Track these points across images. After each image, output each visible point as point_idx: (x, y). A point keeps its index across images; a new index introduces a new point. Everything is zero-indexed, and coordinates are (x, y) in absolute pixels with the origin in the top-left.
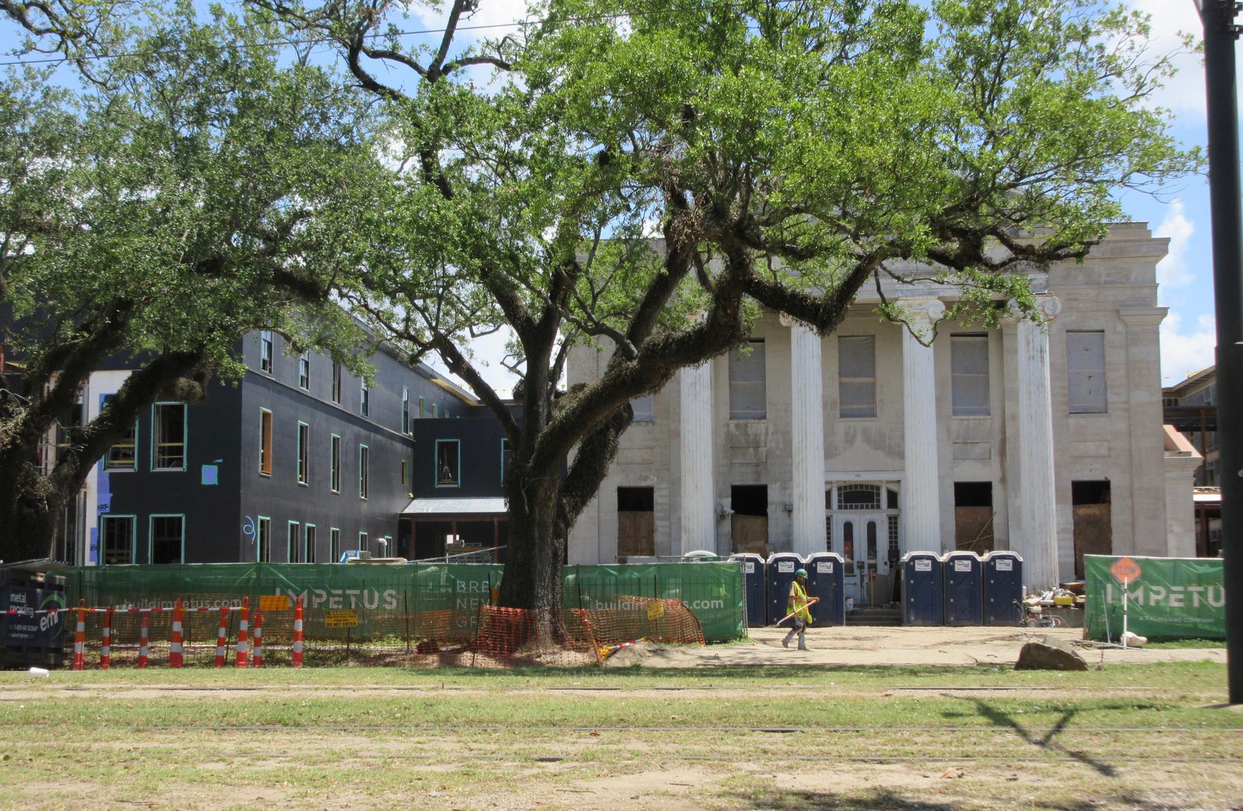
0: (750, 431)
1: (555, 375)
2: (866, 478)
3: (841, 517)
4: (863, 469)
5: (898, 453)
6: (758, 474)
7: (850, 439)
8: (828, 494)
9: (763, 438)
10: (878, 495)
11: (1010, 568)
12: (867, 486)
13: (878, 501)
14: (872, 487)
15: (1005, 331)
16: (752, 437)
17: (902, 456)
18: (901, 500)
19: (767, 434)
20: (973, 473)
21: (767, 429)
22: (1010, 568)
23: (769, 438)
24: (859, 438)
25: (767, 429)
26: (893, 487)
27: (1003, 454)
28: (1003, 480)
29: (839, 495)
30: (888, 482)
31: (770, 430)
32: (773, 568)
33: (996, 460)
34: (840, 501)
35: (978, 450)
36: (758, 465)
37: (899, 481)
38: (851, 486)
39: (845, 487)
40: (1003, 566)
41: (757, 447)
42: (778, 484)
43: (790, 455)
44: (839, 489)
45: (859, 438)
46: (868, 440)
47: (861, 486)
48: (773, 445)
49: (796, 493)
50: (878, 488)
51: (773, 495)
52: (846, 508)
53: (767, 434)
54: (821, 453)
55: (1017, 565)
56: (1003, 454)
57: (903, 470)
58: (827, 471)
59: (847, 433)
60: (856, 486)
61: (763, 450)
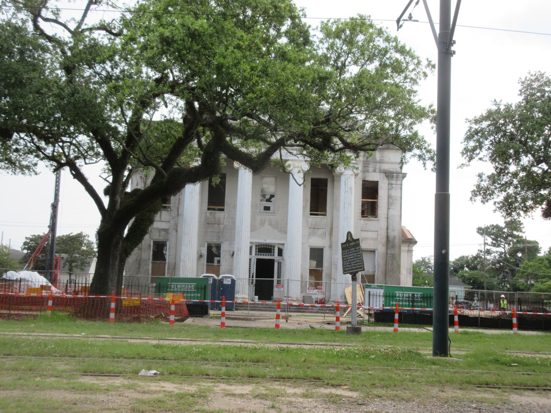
0: (216, 216)
1: (125, 185)
2: (269, 241)
4: (268, 238)
5: (283, 229)
6: (219, 237)
7: (262, 223)
8: (251, 248)
9: (222, 220)
10: (274, 250)
11: (230, 283)
12: (269, 246)
13: (274, 252)
14: (271, 246)
15: (335, 178)
16: (217, 219)
17: (285, 232)
18: (285, 253)
19: (224, 218)
20: (317, 242)
21: (224, 216)
22: (230, 283)
23: (225, 220)
24: (267, 223)
25: (224, 216)
26: (281, 247)
27: (331, 234)
28: (330, 247)
29: (256, 249)
30: (279, 244)
31: (226, 217)
32: (221, 281)
33: (328, 236)
34: (256, 252)
35: (320, 231)
36: (219, 233)
37: (284, 244)
38: (261, 245)
39: (259, 246)
40: (227, 282)
41: (219, 224)
42: (228, 242)
43: (235, 228)
44: (256, 246)
45: (267, 223)
46: (270, 224)
47: (266, 245)
48: (227, 223)
49: (236, 246)
50: (274, 247)
51: (224, 248)
53: (224, 218)
54: (249, 229)
55: (233, 281)
56: (331, 234)
57: (285, 239)
58: (251, 237)
59: (261, 220)
60: (264, 245)
61: (222, 226)
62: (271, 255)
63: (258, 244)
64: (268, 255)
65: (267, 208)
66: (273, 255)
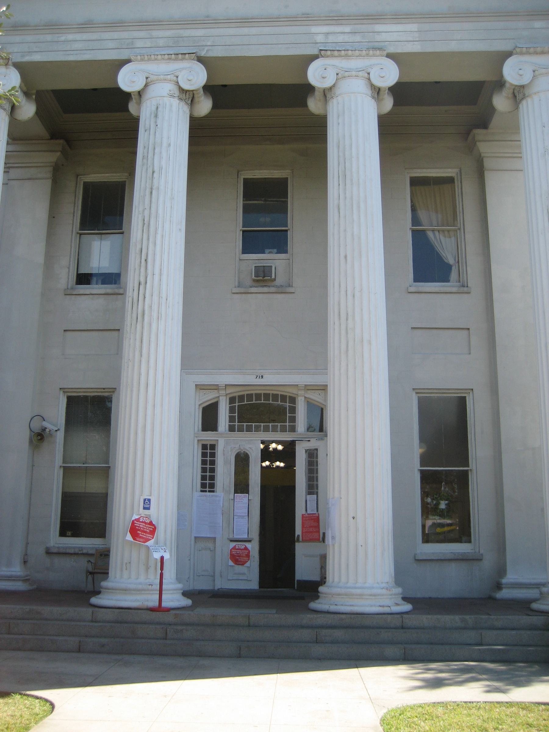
2: (274, 378)
3: (229, 443)
10: (293, 410)
12: (275, 397)
13: (293, 420)
14: (284, 398)
15: (487, 163)
26: (316, 397)
29: (232, 410)
30: (308, 388)
34: (232, 419)
38: (250, 396)
39: (241, 398)
44: (232, 400)
47: (267, 396)
50: (293, 400)
52: (240, 430)
60: (258, 396)
62: (283, 430)
63: (235, 392)
64: (275, 430)
65: (263, 276)
66: (293, 429)
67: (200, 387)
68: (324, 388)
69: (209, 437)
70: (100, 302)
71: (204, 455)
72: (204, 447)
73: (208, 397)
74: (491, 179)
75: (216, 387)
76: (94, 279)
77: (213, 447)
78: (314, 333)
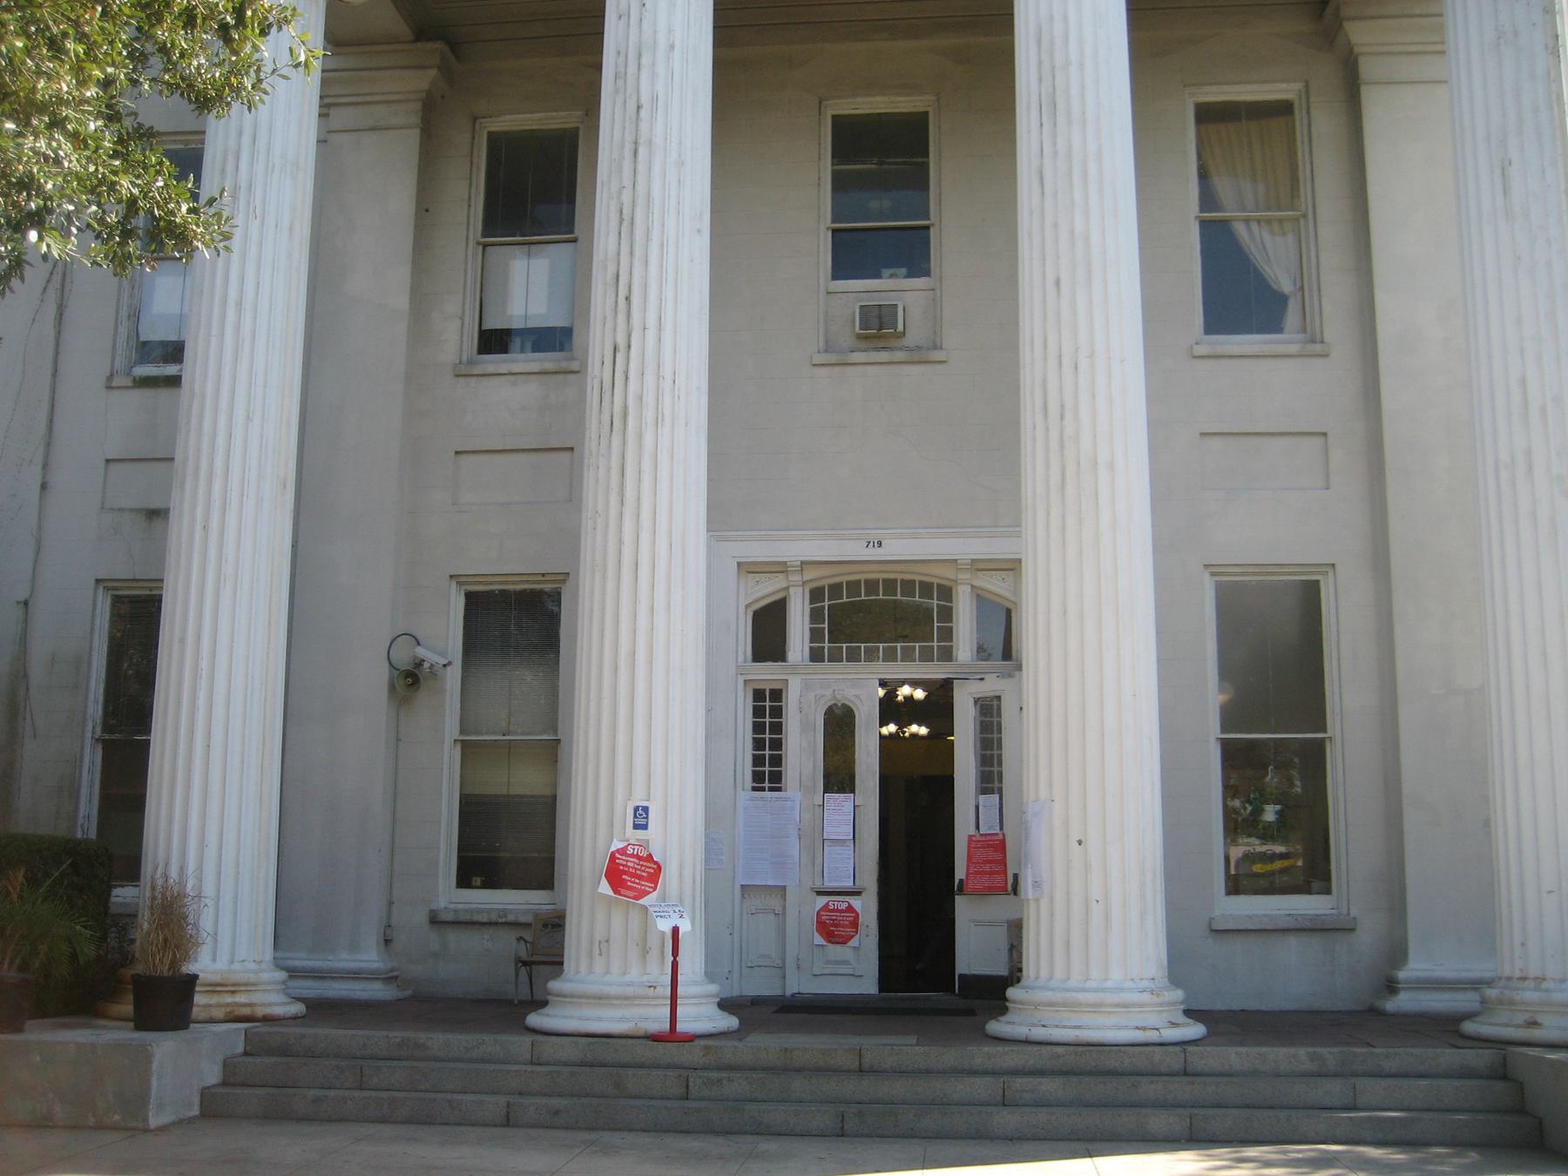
2: (906, 546)
3: (809, 689)
10: (947, 614)
12: (908, 586)
13: (947, 634)
14: (926, 588)
15: (1367, 68)
26: (995, 585)
29: (816, 615)
34: (816, 635)
38: (854, 586)
39: (835, 589)
44: (816, 595)
47: (890, 585)
50: (946, 593)
52: (835, 657)
60: (872, 586)
62: (927, 656)
64: (908, 656)
65: (878, 327)
66: (947, 655)
67: (747, 569)
68: (1013, 567)
69: (768, 673)
70: (533, 388)
71: (758, 712)
72: (758, 695)
73: (765, 590)
74: (1377, 107)
75: (781, 568)
76: (516, 342)
77: (777, 695)
78: (989, 443)
